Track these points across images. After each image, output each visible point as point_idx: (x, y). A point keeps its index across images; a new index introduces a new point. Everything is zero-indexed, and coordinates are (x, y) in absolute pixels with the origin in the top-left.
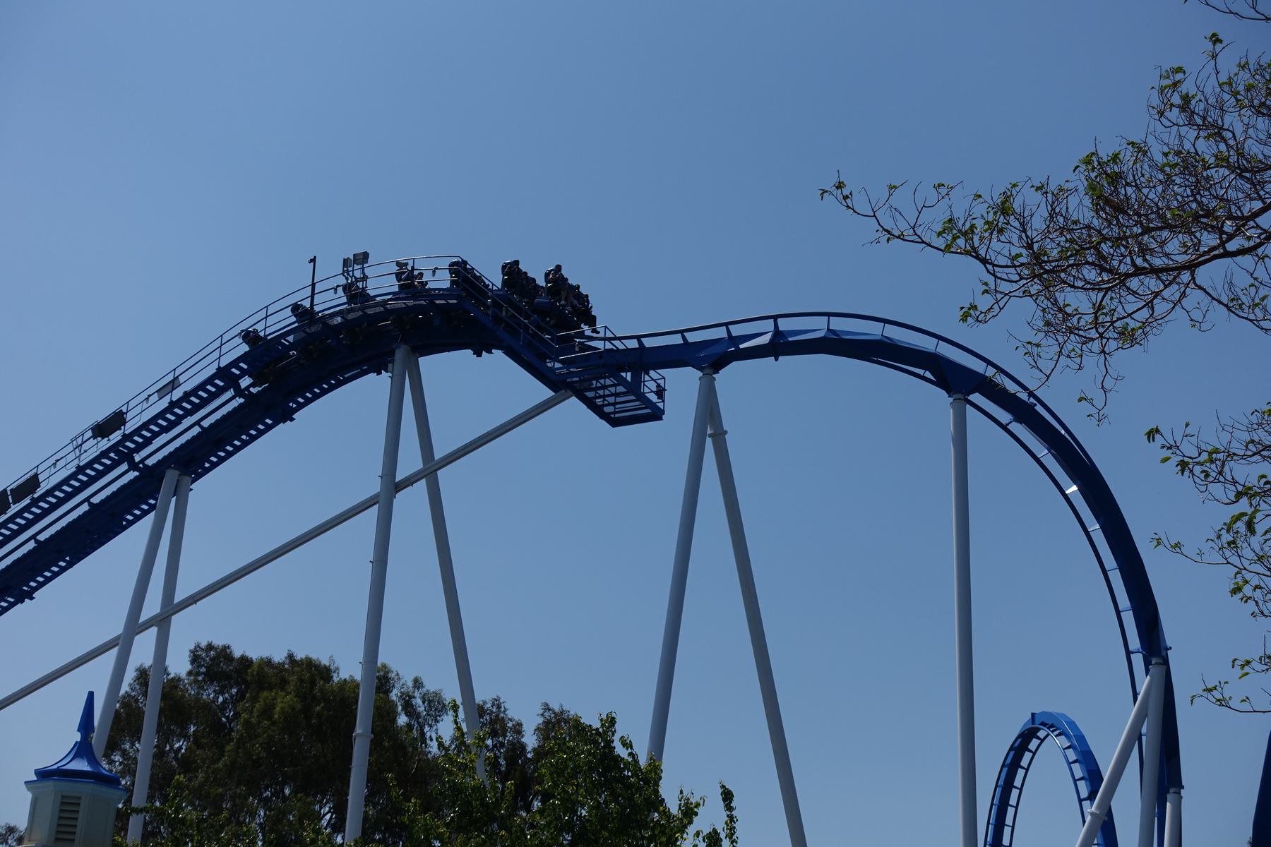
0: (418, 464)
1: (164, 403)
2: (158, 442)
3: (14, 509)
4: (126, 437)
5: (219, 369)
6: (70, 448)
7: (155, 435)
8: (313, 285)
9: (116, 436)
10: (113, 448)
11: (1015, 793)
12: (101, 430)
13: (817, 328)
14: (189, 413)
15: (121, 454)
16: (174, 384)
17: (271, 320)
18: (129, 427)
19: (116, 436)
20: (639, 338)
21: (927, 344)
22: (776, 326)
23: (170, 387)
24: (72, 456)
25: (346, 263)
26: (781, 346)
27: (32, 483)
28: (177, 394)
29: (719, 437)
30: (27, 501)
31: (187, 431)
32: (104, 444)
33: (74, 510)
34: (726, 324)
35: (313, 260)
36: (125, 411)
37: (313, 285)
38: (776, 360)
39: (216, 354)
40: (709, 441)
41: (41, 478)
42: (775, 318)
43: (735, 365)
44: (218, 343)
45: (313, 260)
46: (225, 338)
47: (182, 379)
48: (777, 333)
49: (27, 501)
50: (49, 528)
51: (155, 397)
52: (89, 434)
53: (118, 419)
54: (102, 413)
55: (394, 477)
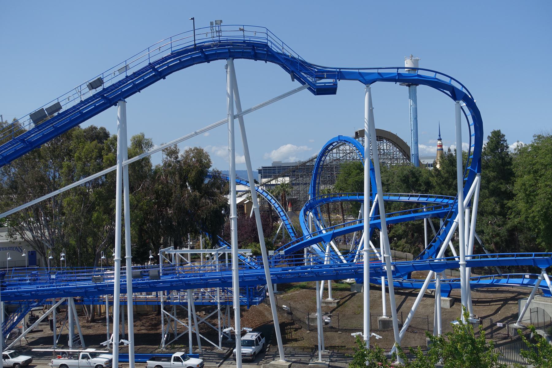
1: (122, 77)
5: (150, 64)
9: (100, 89)
12: (92, 86)
16: (126, 68)
18: (106, 85)
20: (340, 69)
21: (447, 80)
23: (125, 69)
24: (76, 96)
25: (212, 23)
28: (129, 73)
35: (193, 19)
36: (102, 77)
41: (61, 104)
43: (377, 82)
45: (193, 19)
47: (130, 66)
52: (85, 86)
53: (99, 82)
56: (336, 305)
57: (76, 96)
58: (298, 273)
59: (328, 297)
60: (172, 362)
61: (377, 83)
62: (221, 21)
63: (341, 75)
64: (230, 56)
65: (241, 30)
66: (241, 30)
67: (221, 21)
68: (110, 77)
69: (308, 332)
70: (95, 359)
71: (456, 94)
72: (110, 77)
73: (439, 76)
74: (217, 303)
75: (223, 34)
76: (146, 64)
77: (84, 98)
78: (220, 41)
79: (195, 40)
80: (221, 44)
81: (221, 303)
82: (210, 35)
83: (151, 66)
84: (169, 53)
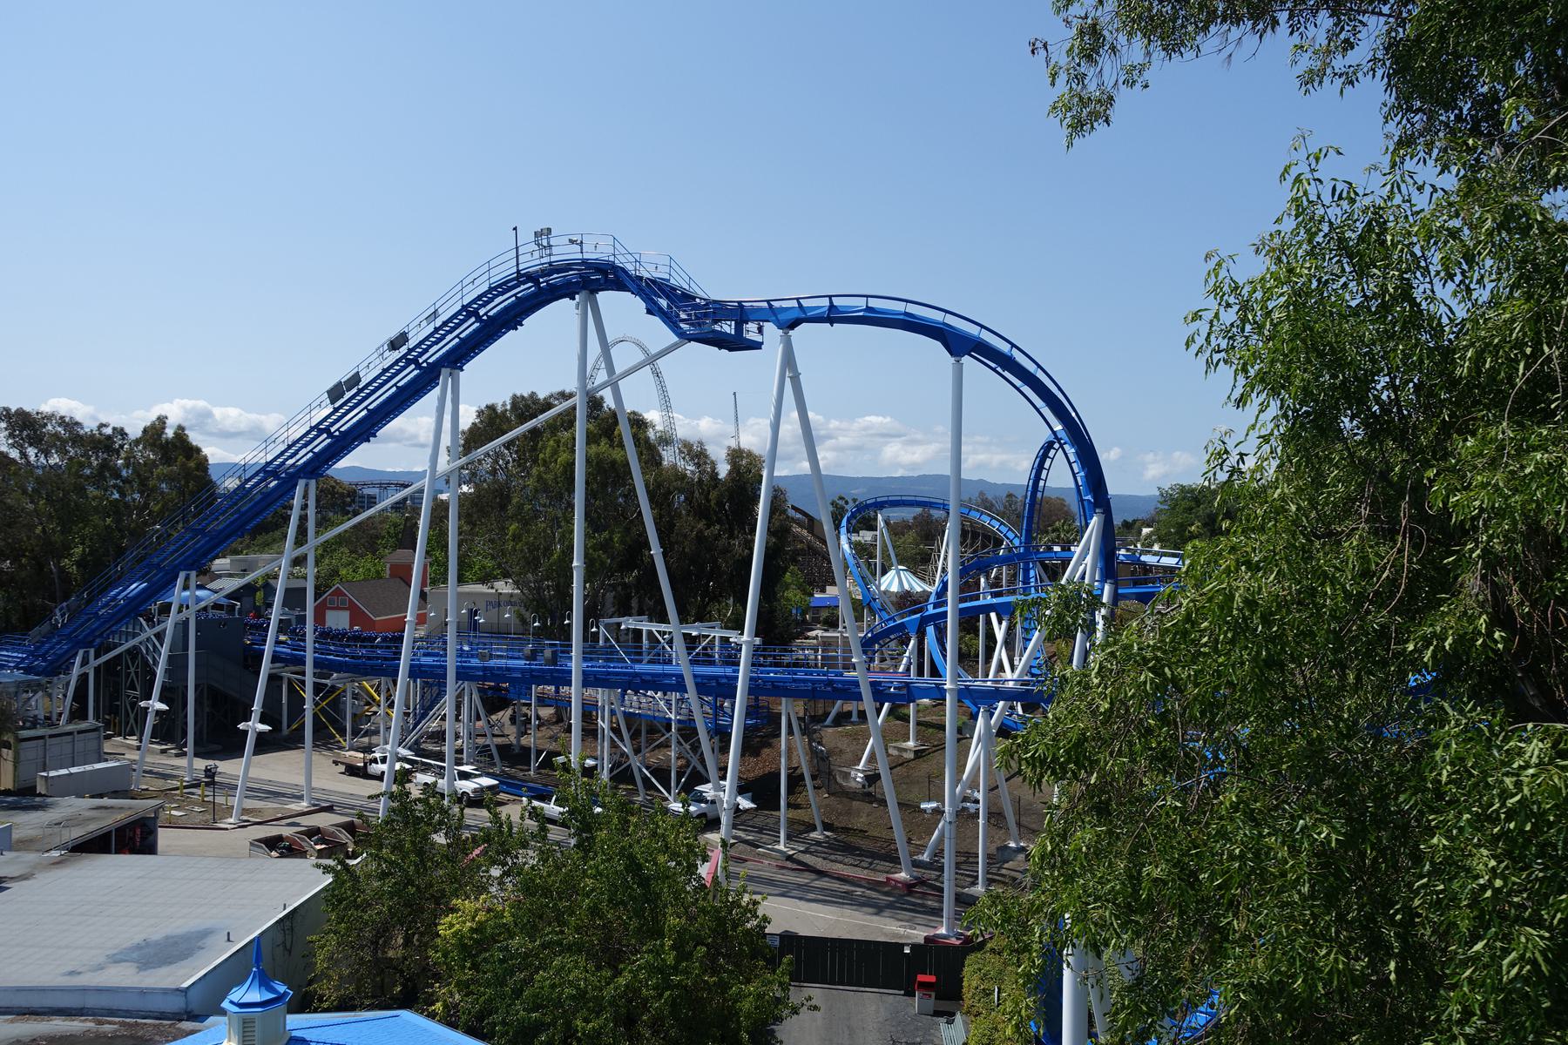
1: (430, 329)
2: (432, 351)
3: (348, 395)
4: (410, 351)
6: (376, 355)
7: (430, 347)
9: (404, 350)
10: (404, 356)
12: (394, 345)
14: (450, 332)
15: (407, 360)
16: (435, 314)
17: (493, 272)
18: (412, 344)
19: (404, 350)
24: (377, 361)
26: (833, 316)
27: (356, 379)
28: (438, 323)
29: (796, 379)
30: (354, 391)
31: (451, 342)
32: (397, 355)
33: (388, 391)
35: (515, 229)
39: (459, 295)
41: (361, 374)
44: (459, 287)
45: (515, 229)
46: (465, 283)
47: (440, 311)
48: (832, 306)
49: (354, 391)
50: (375, 402)
51: (424, 323)
52: (386, 347)
53: (402, 338)
54: (393, 333)
56: (912, 756)
57: (377, 361)
58: (814, 682)
59: (909, 739)
60: (552, 805)
62: (549, 230)
63: (741, 314)
64: (584, 288)
65: (572, 242)
66: (572, 242)
67: (549, 230)
68: (415, 331)
70: (464, 783)
71: (957, 344)
72: (415, 331)
73: (912, 309)
74: (670, 719)
75: (555, 250)
76: (458, 307)
77: (386, 364)
78: (550, 263)
80: (552, 269)
81: (679, 721)
82: (536, 255)
83: (468, 311)
84: (485, 288)
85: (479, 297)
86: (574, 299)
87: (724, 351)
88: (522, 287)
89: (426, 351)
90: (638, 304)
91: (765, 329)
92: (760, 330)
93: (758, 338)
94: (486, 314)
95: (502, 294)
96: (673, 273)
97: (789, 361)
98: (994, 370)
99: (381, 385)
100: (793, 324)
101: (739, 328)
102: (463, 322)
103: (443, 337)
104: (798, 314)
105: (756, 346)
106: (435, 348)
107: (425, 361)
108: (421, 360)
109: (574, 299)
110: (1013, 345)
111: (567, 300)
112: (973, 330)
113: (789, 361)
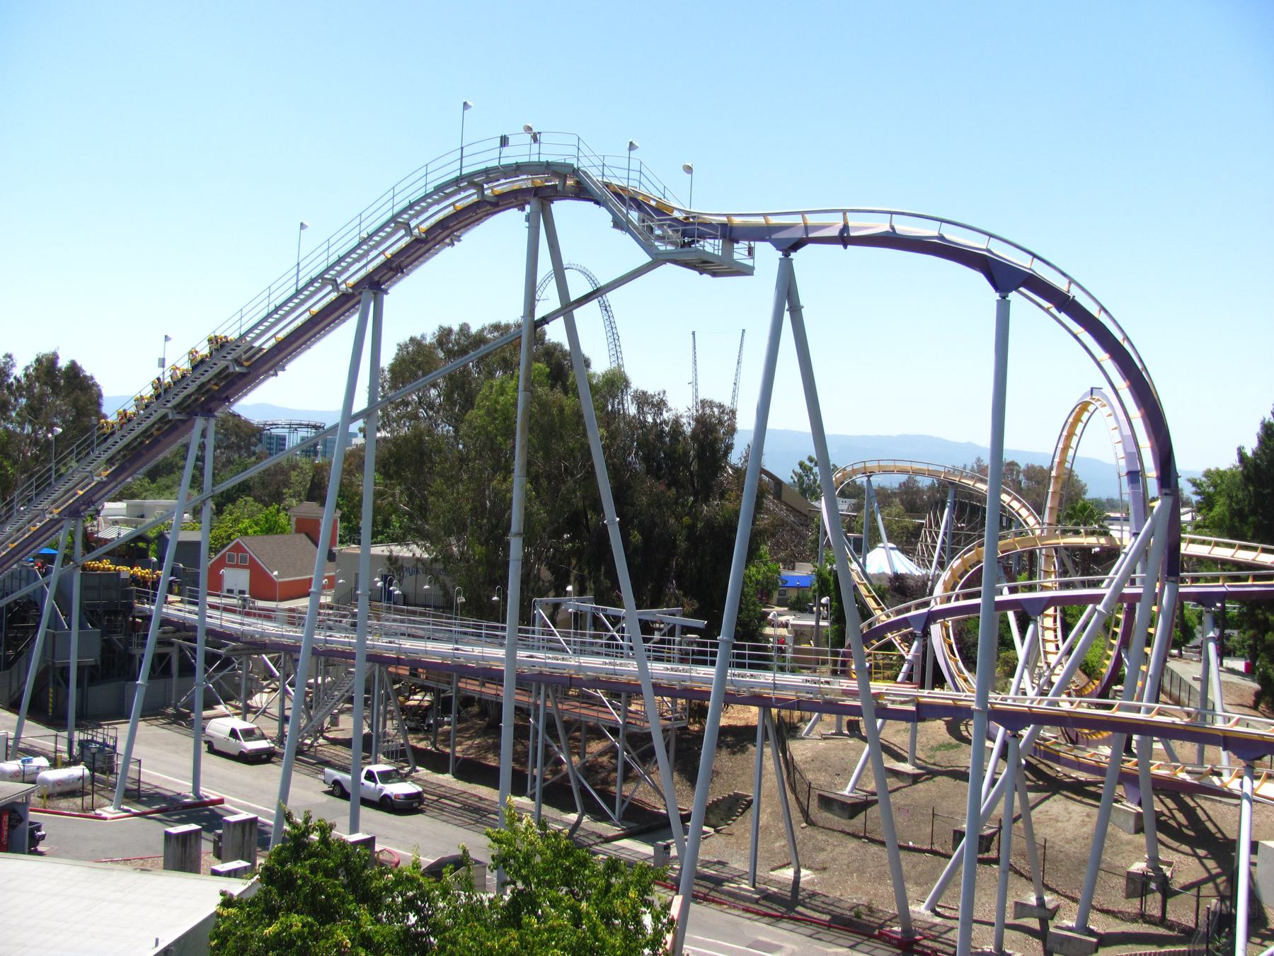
0: (556, 304)
7: (351, 264)
8: (462, 148)
11: (1080, 426)
13: (880, 226)
17: (430, 178)
22: (845, 219)
29: (796, 311)
34: (802, 213)
37: (462, 148)
38: (845, 248)
40: (787, 315)
42: (844, 212)
48: (846, 228)
55: (533, 316)
61: (809, 248)
63: (729, 233)
69: (804, 825)
79: (461, 167)
83: (397, 222)
85: (411, 206)
86: (523, 209)
87: (706, 277)
88: (463, 195)
89: (346, 269)
90: (602, 216)
91: (757, 253)
92: (751, 252)
93: (749, 262)
94: (417, 226)
95: (437, 202)
96: (643, 180)
97: (788, 294)
98: (1047, 310)
99: (293, 310)
100: (797, 245)
101: (728, 251)
102: (390, 235)
103: (367, 253)
104: (800, 234)
105: (746, 271)
106: (357, 266)
107: (344, 282)
108: (339, 281)
109: (523, 209)
110: (1071, 281)
111: (515, 210)
112: (1021, 261)
113: (788, 294)
